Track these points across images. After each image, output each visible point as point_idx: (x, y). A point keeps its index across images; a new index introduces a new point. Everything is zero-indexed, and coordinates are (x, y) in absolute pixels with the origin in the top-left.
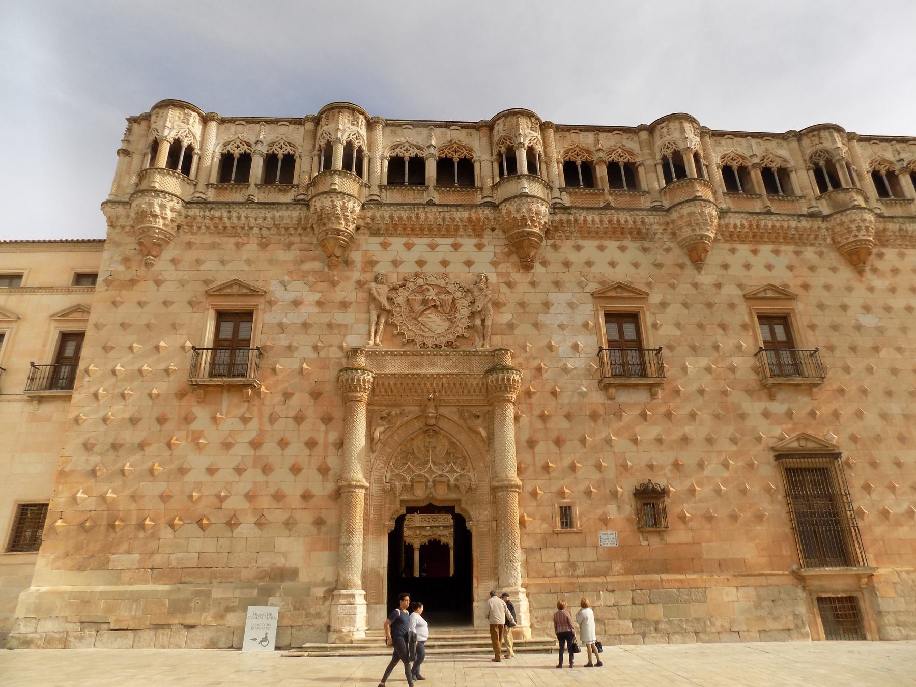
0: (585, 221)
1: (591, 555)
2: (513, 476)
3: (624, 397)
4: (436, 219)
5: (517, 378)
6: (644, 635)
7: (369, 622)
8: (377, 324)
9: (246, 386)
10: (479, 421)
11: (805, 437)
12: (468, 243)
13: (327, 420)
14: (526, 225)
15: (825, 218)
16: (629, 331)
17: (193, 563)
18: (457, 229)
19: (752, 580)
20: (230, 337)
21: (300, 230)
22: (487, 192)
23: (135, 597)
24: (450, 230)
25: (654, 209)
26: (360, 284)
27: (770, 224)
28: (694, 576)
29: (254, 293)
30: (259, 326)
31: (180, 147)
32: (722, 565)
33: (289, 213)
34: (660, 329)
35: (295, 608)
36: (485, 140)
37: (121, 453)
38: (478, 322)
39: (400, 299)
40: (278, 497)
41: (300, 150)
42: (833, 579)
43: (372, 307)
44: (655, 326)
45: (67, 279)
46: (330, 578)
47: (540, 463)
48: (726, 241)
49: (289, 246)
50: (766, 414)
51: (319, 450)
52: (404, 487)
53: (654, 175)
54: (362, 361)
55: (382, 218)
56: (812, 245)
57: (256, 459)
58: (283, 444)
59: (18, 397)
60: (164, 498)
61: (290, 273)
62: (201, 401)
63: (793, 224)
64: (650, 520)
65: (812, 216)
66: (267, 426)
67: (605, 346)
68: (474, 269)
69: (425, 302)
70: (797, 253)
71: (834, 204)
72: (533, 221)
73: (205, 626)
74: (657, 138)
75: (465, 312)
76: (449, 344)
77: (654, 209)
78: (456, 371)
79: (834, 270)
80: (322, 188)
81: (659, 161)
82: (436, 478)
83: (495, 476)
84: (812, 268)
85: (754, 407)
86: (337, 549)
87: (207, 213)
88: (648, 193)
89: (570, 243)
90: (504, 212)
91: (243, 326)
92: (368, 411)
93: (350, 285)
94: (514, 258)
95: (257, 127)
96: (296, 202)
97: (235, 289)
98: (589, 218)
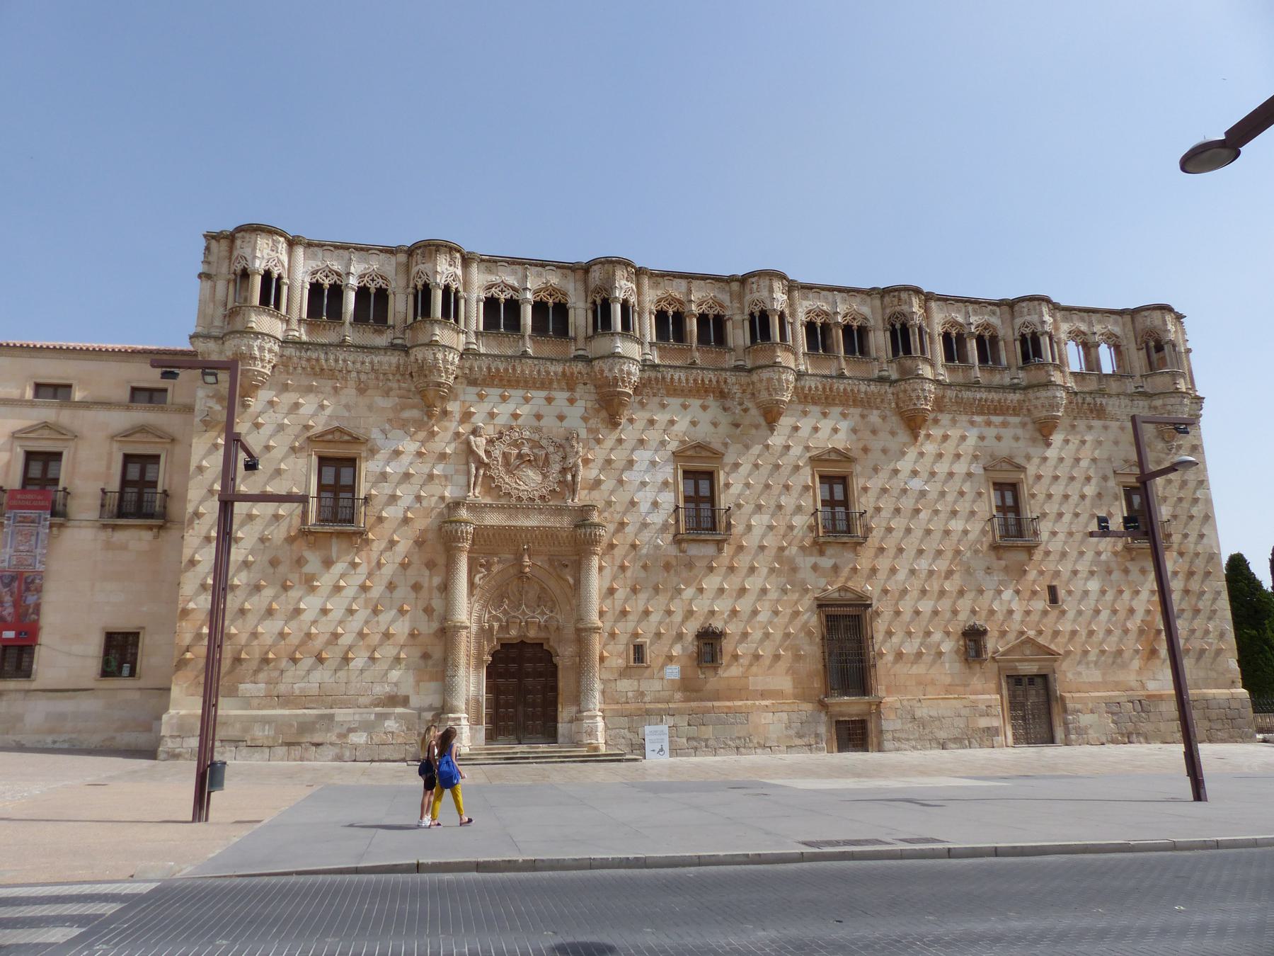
0: (672, 378)
1: (657, 685)
2: (595, 619)
3: (694, 550)
4: (531, 371)
5: (603, 533)
6: (696, 749)
7: (472, 738)
8: (476, 476)
9: (355, 533)
10: (567, 570)
12: (561, 396)
13: (430, 565)
14: (616, 385)
15: (892, 383)
16: (704, 486)
17: (315, 691)
18: (551, 382)
19: (786, 708)
20: (332, 482)
21: (398, 377)
22: (581, 343)
23: (265, 721)
24: (544, 384)
25: (737, 369)
27: (842, 388)
28: (740, 703)
29: (356, 440)
30: (363, 474)
31: (271, 279)
33: (387, 358)
34: (733, 488)
35: (408, 729)
36: (580, 286)
38: (569, 477)
39: (497, 453)
41: (393, 284)
42: (850, 705)
43: (471, 459)
44: (727, 485)
45: (125, 395)
46: (437, 704)
47: (618, 608)
48: (800, 402)
49: (387, 393)
50: (815, 567)
51: (424, 593)
52: (500, 626)
53: (740, 332)
54: (464, 513)
55: (480, 368)
56: (877, 408)
61: (390, 421)
62: (313, 546)
63: (863, 387)
64: (708, 658)
65: (882, 380)
67: (681, 504)
68: (566, 423)
70: (863, 416)
72: (623, 381)
73: (331, 744)
74: (747, 291)
75: (556, 468)
76: (542, 498)
77: (737, 369)
78: (549, 524)
79: (893, 433)
80: (423, 338)
81: (747, 317)
82: (530, 623)
83: (580, 619)
84: (874, 432)
85: (806, 562)
86: (443, 679)
87: (303, 354)
88: (733, 350)
89: (657, 399)
90: (597, 369)
91: (346, 473)
92: (469, 558)
94: (604, 414)
95: (346, 253)
96: (393, 347)
97: (337, 435)
98: (676, 377)
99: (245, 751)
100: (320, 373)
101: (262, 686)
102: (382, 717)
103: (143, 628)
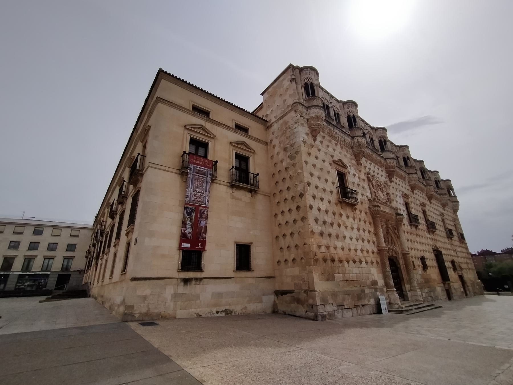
11: (436, 246)
13: (370, 223)
15: (426, 186)
26: (365, 173)
32: (434, 280)
37: (326, 226)
40: (368, 252)
43: (370, 184)
57: (360, 235)
58: (364, 230)
66: (359, 223)
69: (378, 186)
71: (426, 183)
75: (385, 193)
85: (428, 236)
93: (363, 174)
99: (345, 311)
100: (331, 136)
101: (341, 275)
102: (376, 290)
103: (252, 243)
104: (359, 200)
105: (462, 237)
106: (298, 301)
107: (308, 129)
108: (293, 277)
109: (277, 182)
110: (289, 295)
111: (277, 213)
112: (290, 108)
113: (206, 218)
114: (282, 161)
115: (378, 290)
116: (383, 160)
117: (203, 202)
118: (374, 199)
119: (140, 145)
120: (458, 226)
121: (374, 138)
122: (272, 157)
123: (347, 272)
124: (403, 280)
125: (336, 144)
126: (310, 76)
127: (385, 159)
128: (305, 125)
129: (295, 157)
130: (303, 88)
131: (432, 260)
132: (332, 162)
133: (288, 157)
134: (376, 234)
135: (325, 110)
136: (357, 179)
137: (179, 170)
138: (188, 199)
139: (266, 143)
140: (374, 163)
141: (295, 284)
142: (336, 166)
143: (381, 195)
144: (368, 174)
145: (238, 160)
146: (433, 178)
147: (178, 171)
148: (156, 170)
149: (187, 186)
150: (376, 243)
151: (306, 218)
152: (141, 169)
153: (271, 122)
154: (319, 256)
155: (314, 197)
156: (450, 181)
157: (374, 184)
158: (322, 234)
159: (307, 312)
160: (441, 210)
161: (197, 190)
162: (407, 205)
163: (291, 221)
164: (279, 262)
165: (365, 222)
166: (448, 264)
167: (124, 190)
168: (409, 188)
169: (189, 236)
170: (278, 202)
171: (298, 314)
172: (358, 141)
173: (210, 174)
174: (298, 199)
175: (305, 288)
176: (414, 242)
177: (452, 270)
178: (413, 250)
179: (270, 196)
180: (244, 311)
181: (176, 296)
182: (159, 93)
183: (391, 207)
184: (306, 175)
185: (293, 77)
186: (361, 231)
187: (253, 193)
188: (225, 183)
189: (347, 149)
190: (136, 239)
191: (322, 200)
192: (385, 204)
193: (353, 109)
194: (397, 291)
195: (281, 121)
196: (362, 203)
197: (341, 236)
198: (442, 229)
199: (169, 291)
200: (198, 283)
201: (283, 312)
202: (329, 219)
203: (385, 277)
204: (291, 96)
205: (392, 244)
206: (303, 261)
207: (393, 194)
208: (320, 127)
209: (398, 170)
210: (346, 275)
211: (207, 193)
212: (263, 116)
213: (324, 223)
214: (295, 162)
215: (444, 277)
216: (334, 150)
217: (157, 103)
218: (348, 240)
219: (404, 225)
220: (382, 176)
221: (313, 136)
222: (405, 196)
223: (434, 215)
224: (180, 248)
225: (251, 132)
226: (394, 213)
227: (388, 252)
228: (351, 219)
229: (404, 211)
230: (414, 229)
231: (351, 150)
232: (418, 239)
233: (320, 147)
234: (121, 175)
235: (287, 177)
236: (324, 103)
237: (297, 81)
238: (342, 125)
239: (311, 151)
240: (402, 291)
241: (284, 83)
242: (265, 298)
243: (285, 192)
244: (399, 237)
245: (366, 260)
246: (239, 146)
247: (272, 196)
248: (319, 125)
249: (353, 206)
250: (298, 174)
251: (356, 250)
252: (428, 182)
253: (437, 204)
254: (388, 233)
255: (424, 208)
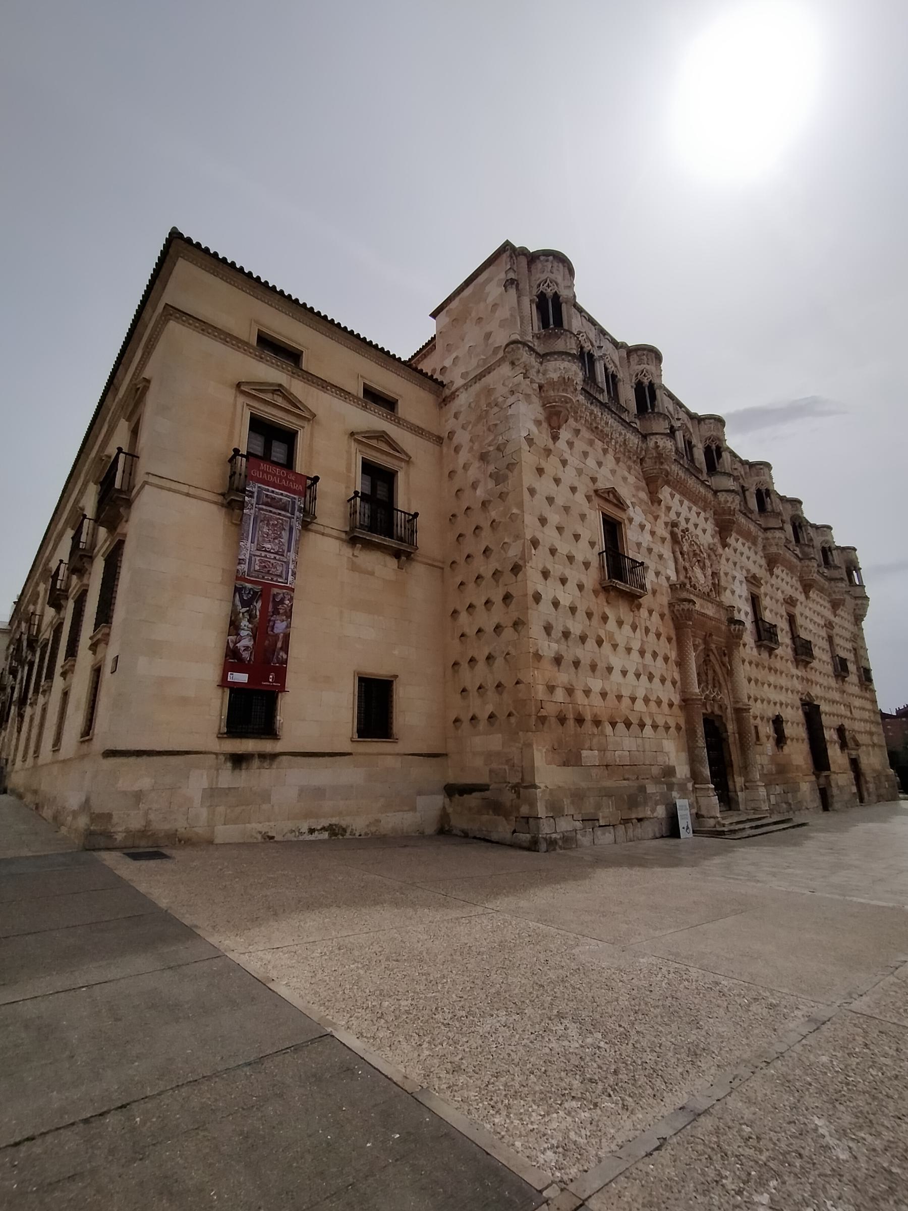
11: (809, 694)
13: (669, 640)
15: (801, 560)
26: (666, 524)
32: (798, 767)
40: (659, 703)
43: (677, 549)
44: (766, 608)
58: (655, 655)
59: (334, 533)
60: (604, 695)
71: (802, 552)
84: (796, 589)
85: (794, 671)
93: (663, 526)
99: (599, 832)
100: (594, 429)
102: (670, 787)
103: (396, 676)
104: (648, 586)
105: (866, 677)
106: (496, 807)
107: (540, 409)
108: (490, 756)
109: (460, 535)
110: (475, 794)
111: (458, 608)
112: (501, 354)
113: (289, 615)
114: (474, 486)
115: (676, 787)
116: (710, 495)
117: (280, 576)
118: (683, 585)
119: (123, 427)
120: (861, 652)
121: (694, 441)
122: (452, 474)
123: (610, 747)
124: (732, 766)
125: (605, 451)
126: (552, 276)
127: (716, 492)
128: (535, 399)
129: (505, 478)
130: (534, 307)
131: (798, 724)
132: (592, 493)
133: (491, 476)
134: (681, 664)
135: (584, 364)
136: (648, 537)
137: (223, 495)
138: (244, 567)
139: (439, 440)
140: (690, 500)
141: (491, 771)
142: (602, 502)
143: (700, 577)
144: (675, 525)
145: (369, 478)
146: (818, 541)
147: (220, 499)
148: (165, 492)
149: (241, 537)
150: (679, 684)
151: (523, 623)
152: (125, 488)
153: (453, 389)
154: (550, 710)
155: (546, 574)
156: (855, 549)
157: (685, 549)
158: (558, 660)
159: (514, 832)
160: (828, 614)
161: (268, 546)
162: (755, 601)
163: (489, 628)
164: (457, 721)
165: (658, 636)
166: (830, 735)
167: (83, 538)
168: (763, 562)
169: (246, 655)
170: (462, 584)
171: (495, 837)
172: (658, 447)
173: (300, 510)
174: (508, 577)
175: (515, 780)
176: (763, 684)
177: (837, 746)
178: (759, 701)
179: (444, 567)
180: (373, 829)
181: (212, 794)
182: (171, 295)
183: (720, 605)
184: (530, 520)
185: (512, 275)
186: (648, 656)
187: (403, 558)
188: (334, 533)
189: (630, 463)
190: (116, 659)
191: (563, 581)
192: (706, 596)
193: (651, 368)
194: (716, 789)
195: (477, 387)
196: (654, 592)
197: (601, 665)
198: (826, 657)
199: (197, 782)
200: (266, 765)
201: (463, 831)
202: (576, 627)
203: (693, 760)
204: (503, 324)
205: (714, 686)
206: (513, 720)
207: (726, 574)
208: (569, 405)
209: (742, 520)
210: (608, 754)
211: (292, 555)
212: (434, 370)
213: (566, 634)
214: (505, 490)
215: (820, 761)
216: (600, 464)
217: (167, 321)
218: (616, 675)
219: (745, 645)
220: (704, 531)
221: (552, 428)
222: (753, 580)
223: (811, 627)
224: (224, 683)
225: (402, 410)
226: (724, 618)
227: (704, 705)
228: (627, 628)
229: (747, 614)
230: (765, 655)
231: (638, 467)
232: (772, 678)
233: (566, 456)
234: (77, 501)
235: (486, 525)
236: (582, 348)
237: (521, 286)
238: (624, 404)
239: (543, 464)
240: (728, 790)
241: (488, 289)
242: (421, 801)
243: (479, 560)
244: (730, 673)
245: (654, 721)
246: (373, 443)
247: (447, 569)
248: (567, 401)
249: (633, 599)
250: (513, 518)
251: (633, 699)
252: (806, 549)
253: (822, 602)
254: (707, 661)
255: (791, 609)
